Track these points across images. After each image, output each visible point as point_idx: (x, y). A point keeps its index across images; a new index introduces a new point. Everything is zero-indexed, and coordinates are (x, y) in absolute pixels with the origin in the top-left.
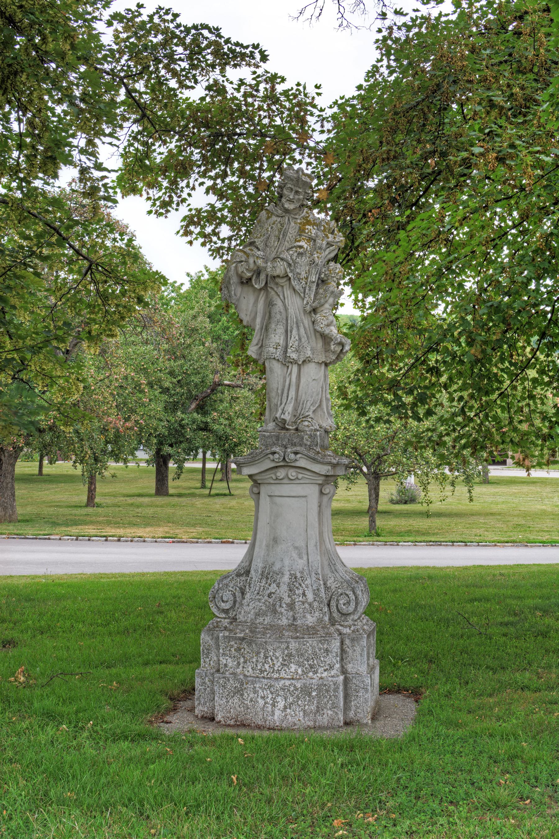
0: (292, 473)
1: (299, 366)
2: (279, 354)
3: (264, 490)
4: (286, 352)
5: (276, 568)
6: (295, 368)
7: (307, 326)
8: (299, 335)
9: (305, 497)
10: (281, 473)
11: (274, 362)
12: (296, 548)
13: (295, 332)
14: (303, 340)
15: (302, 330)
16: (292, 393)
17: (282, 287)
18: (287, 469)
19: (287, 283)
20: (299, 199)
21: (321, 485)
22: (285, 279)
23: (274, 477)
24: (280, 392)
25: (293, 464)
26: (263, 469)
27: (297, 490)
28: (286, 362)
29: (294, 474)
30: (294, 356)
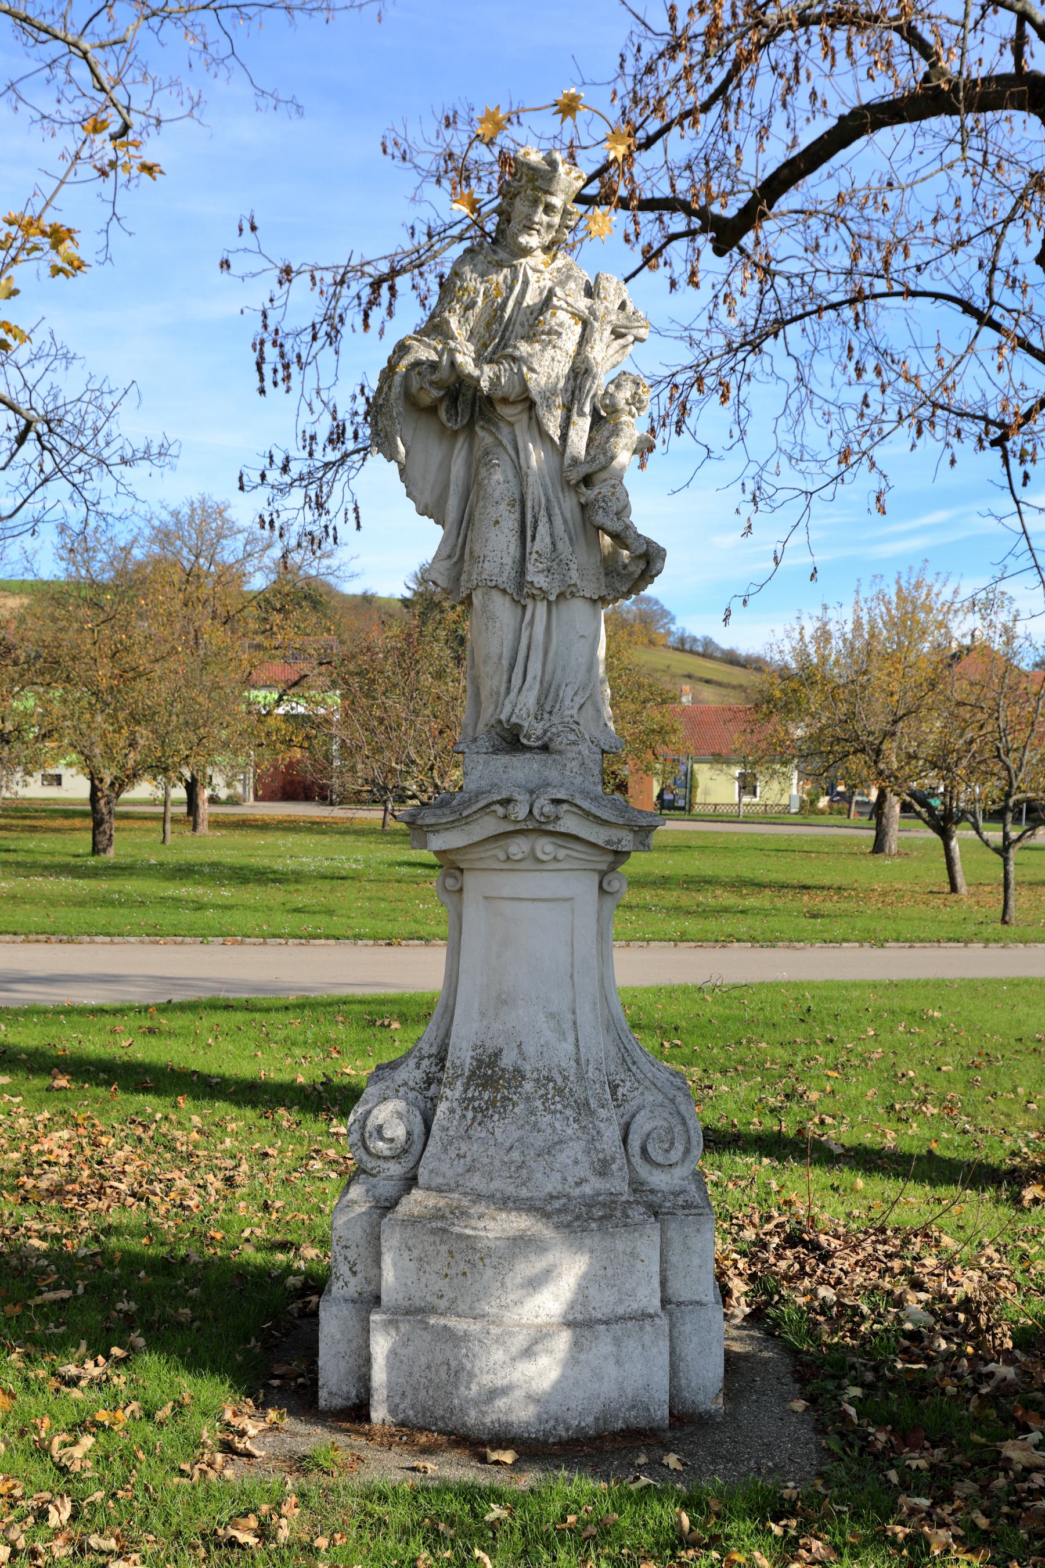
0: (545, 847)
1: (549, 603)
2: (506, 576)
3: (470, 881)
4: (522, 571)
5: (507, 1061)
6: (542, 608)
7: (568, 516)
8: (552, 535)
9: (571, 899)
10: (518, 847)
11: (496, 595)
12: (552, 1015)
13: (543, 529)
14: (560, 545)
15: (558, 521)
16: (535, 668)
17: (511, 424)
18: (532, 837)
19: (525, 417)
20: (550, 226)
21: (603, 874)
22: (520, 407)
23: (502, 856)
24: (505, 662)
25: (550, 828)
26: (476, 839)
27: (550, 884)
28: (521, 593)
29: (549, 848)
30: (540, 581)
